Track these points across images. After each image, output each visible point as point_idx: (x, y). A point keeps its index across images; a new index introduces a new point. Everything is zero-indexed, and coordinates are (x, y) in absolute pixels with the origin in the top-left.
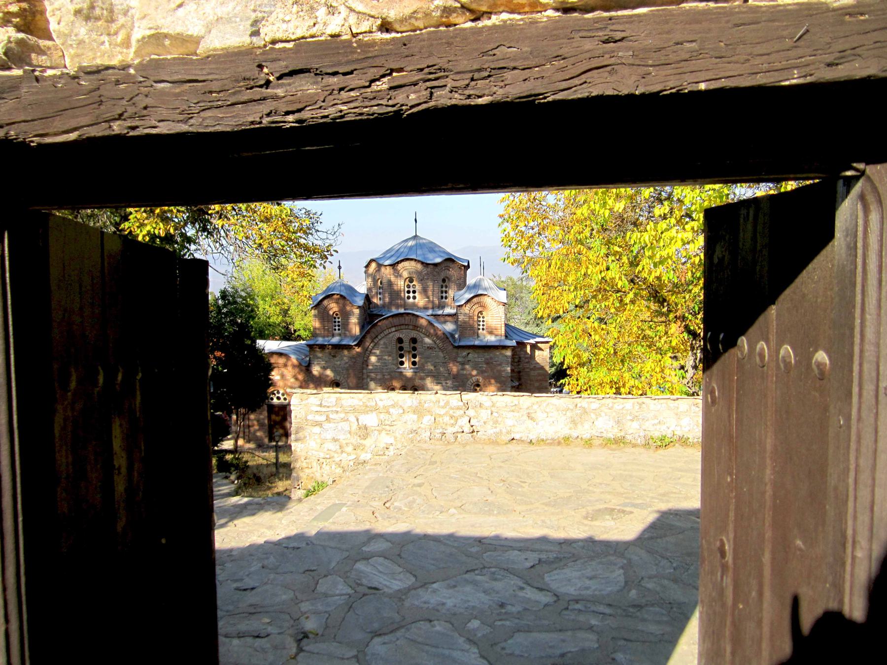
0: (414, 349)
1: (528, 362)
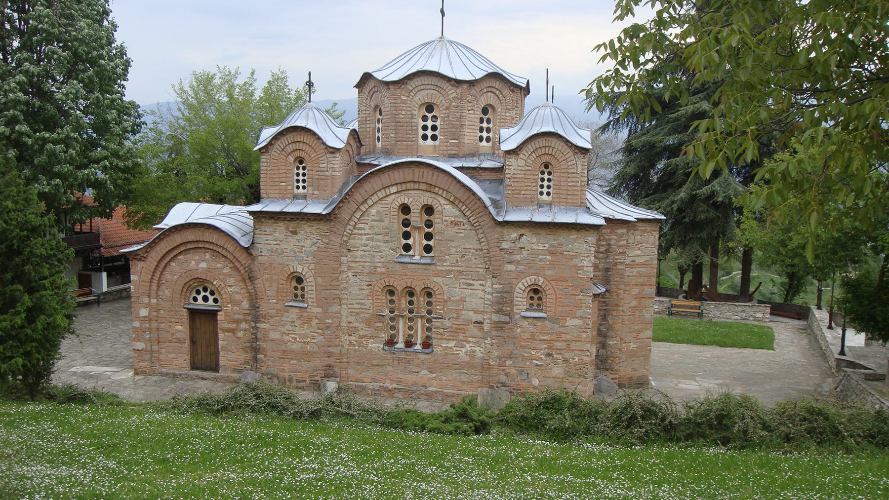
0: (429, 224)
1: (623, 253)
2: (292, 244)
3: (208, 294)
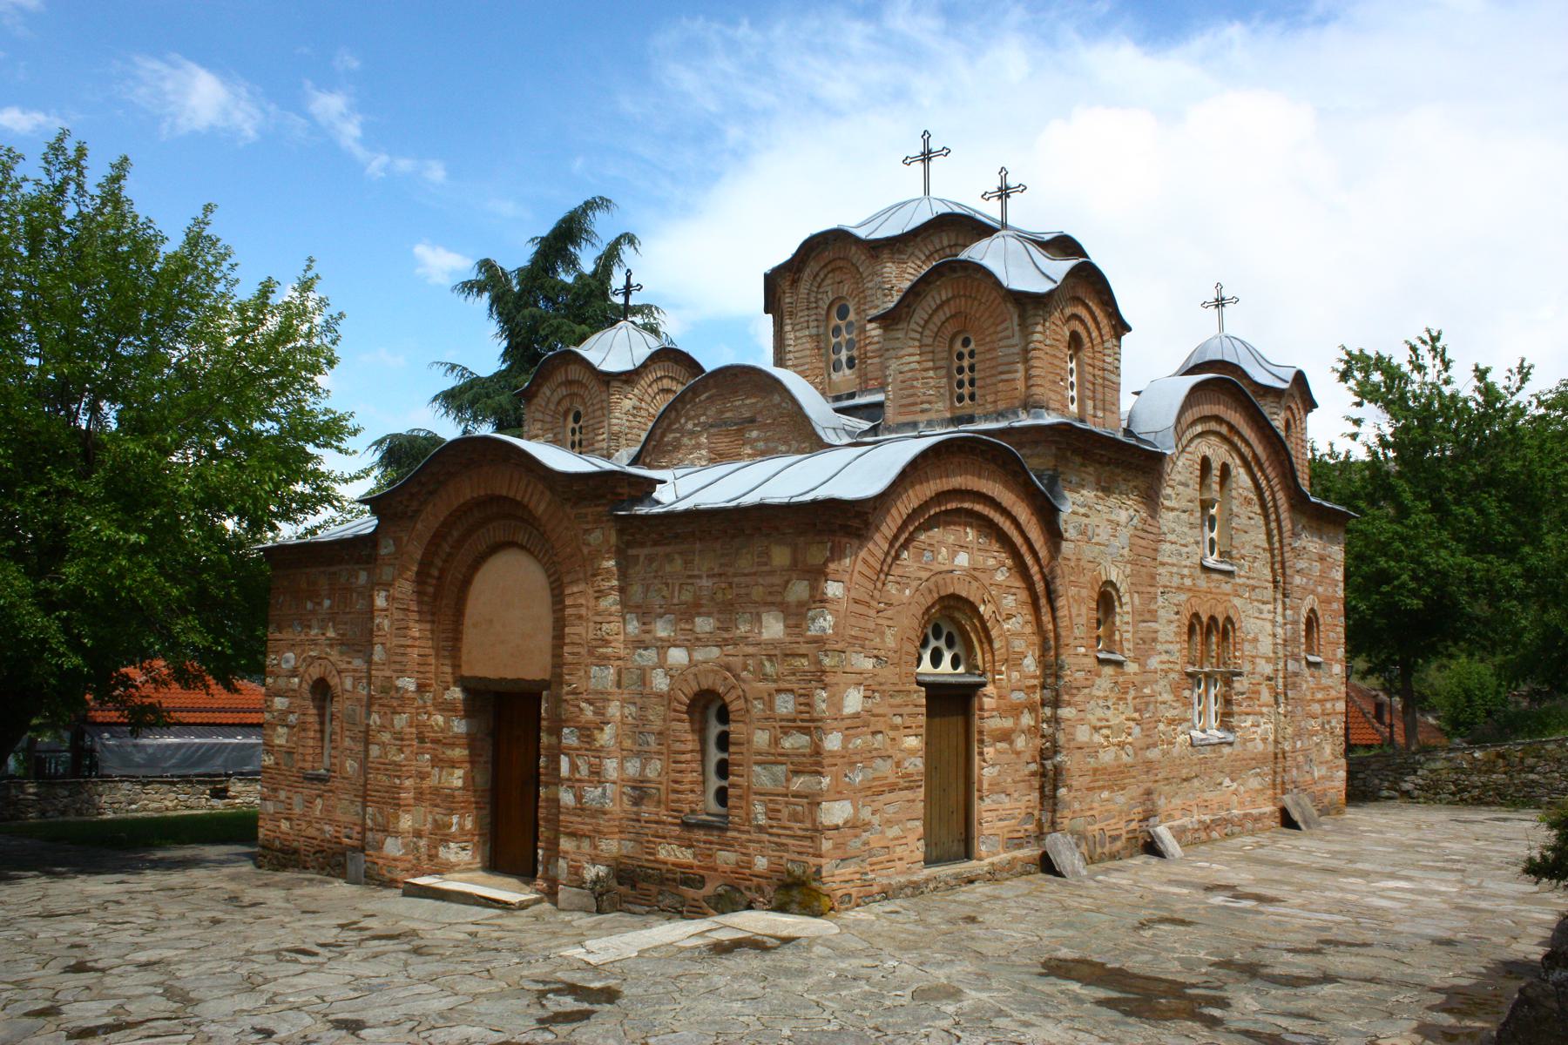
2: (1106, 517)
3: (942, 643)
